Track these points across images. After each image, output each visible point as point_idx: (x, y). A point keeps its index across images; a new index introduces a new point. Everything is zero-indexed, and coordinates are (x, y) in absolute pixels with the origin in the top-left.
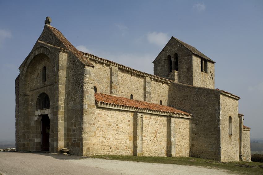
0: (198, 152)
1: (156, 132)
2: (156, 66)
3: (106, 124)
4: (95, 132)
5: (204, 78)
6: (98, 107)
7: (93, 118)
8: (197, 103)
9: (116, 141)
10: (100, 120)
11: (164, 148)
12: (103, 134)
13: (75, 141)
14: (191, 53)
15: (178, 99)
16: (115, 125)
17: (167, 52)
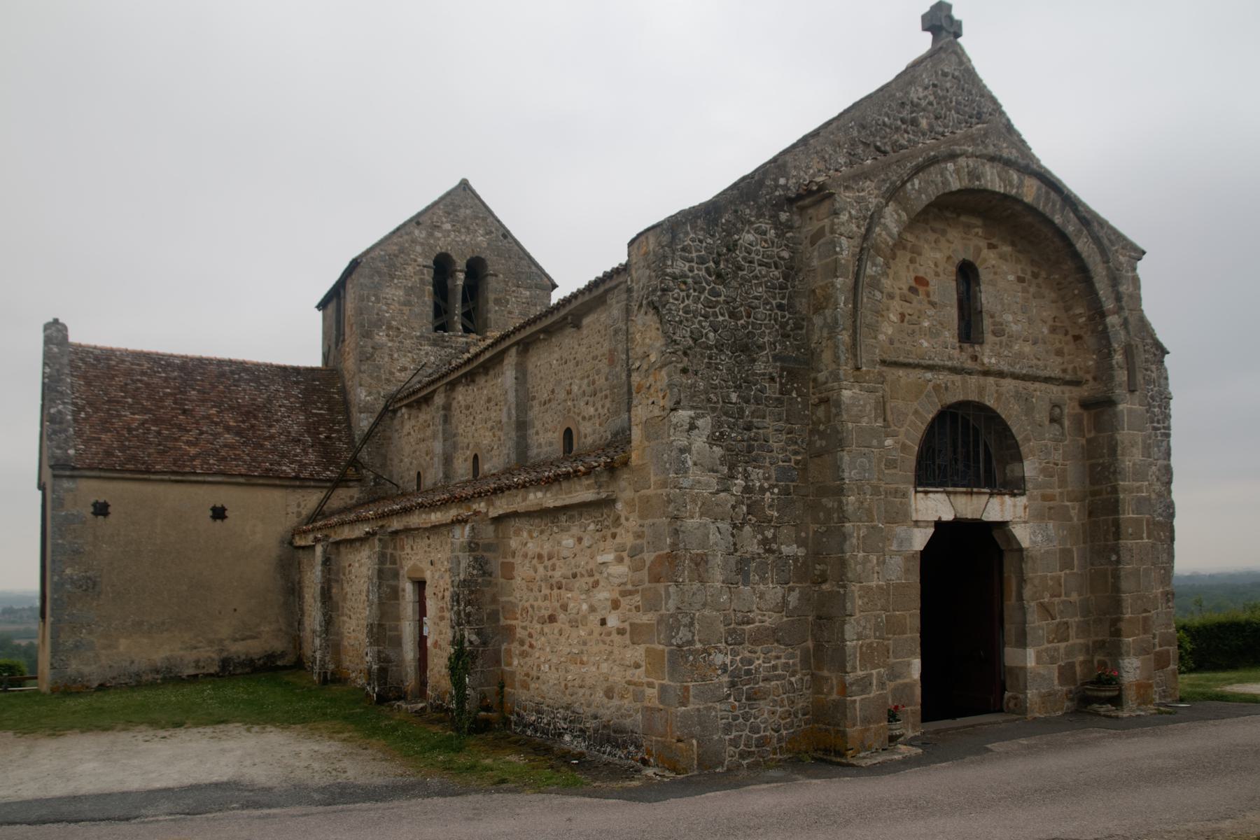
14: (546, 279)
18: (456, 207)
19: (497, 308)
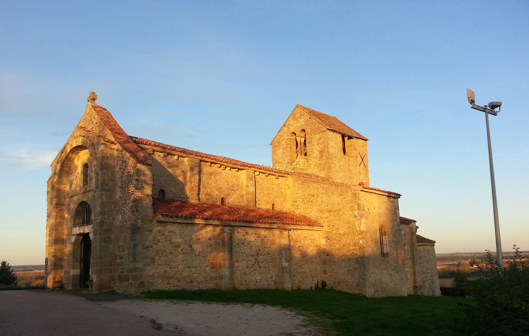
0: (332, 282)
1: (257, 254)
2: (275, 148)
3: (172, 245)
4: (153, 259)
5: (349, 165)
6: (158, 222)
7: (150, 238)
8: (327, 206)
9: (187, 270)
10: (161, 241)
11: (272, 278)
12: (166, 261)
13: (123, 272)
15: (301, 200)
16: (187, 246)
17: (291, 128)
18: (295, 115)
19: (309, 145)
